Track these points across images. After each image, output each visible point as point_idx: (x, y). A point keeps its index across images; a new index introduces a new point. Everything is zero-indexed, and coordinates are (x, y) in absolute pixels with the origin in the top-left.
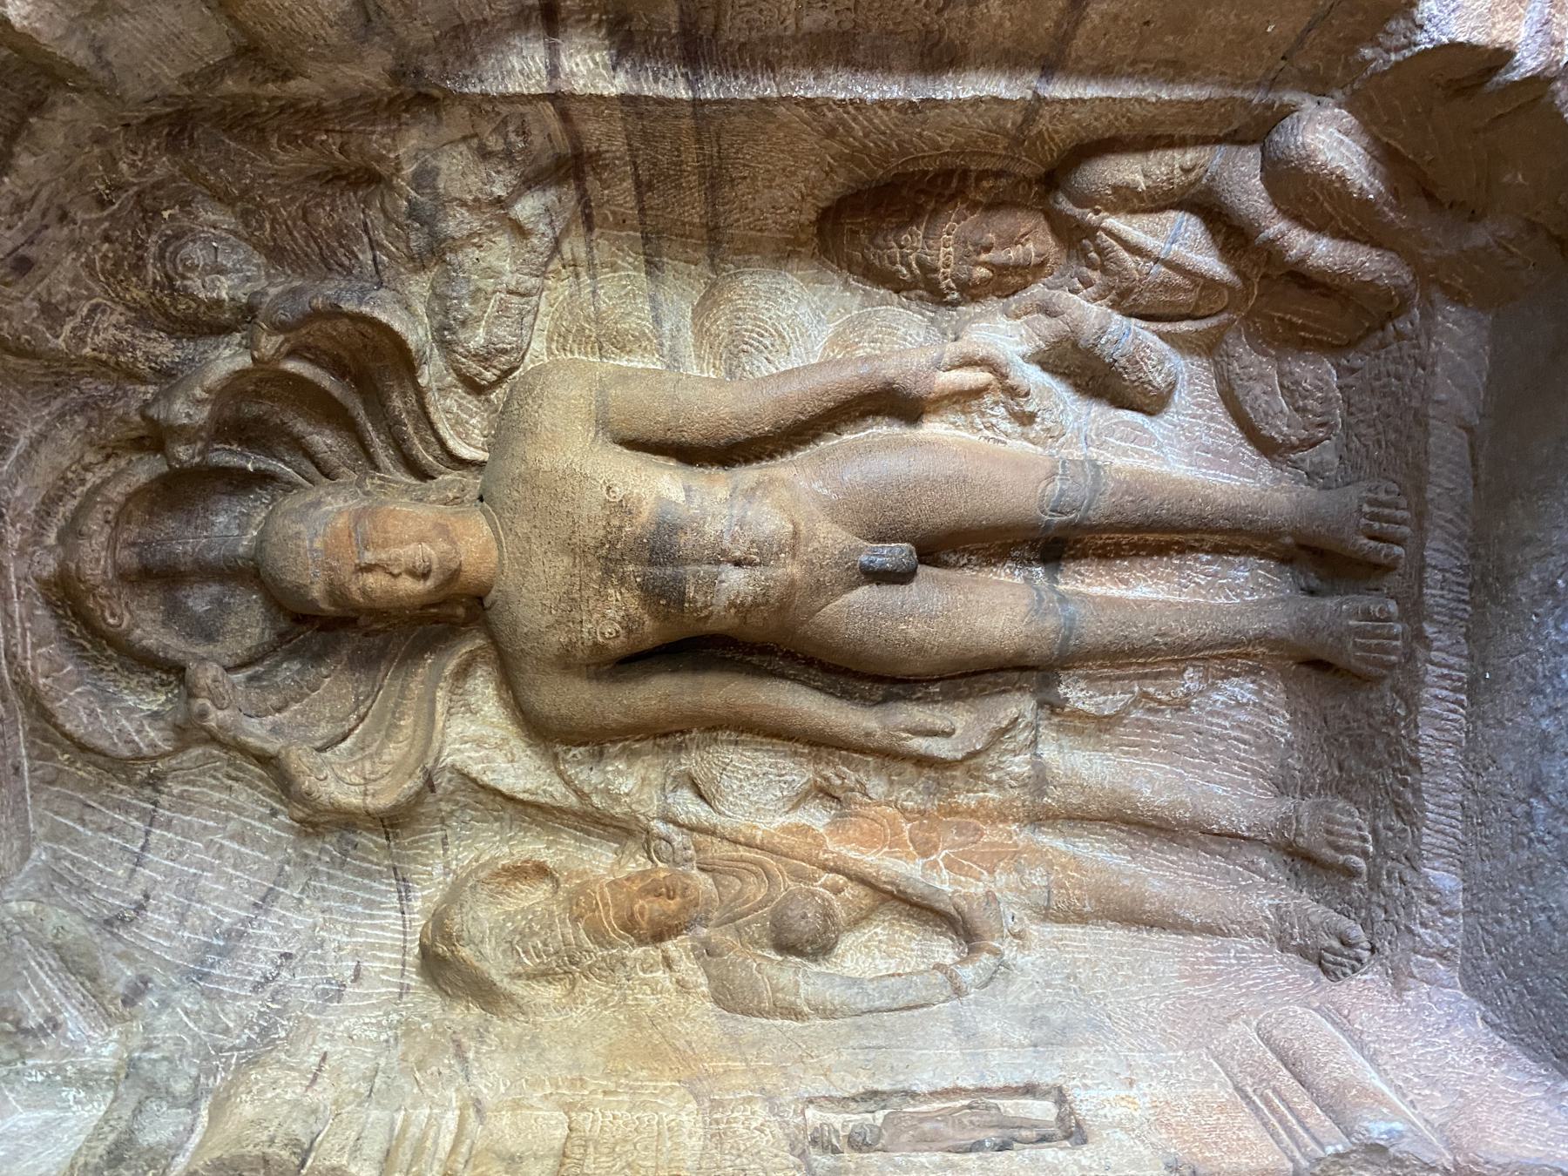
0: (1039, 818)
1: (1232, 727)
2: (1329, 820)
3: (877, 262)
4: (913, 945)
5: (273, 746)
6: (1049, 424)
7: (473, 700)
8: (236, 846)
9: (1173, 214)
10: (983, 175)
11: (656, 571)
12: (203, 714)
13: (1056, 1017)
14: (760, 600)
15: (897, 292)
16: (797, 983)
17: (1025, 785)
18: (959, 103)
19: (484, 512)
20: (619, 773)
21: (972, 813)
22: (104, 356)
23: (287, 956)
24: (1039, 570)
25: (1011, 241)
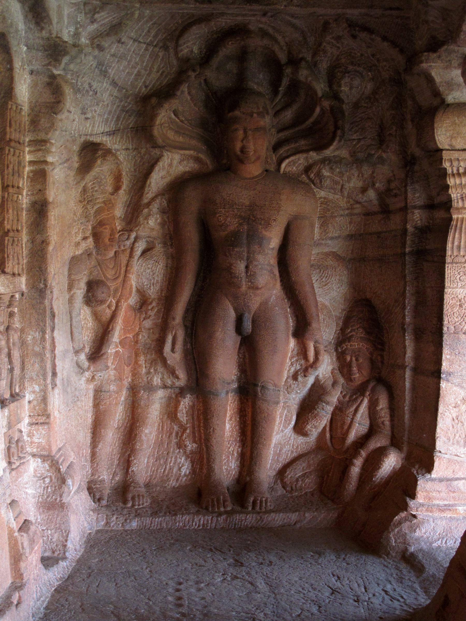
0: (134, 390)
1: (170, 466)
2: (143, 496)
3: (352, 320)
4: (86, 337)
5: (178, 93)
6: (293, 386)
7: (185, 162)
8: (135, 72)
9: (368, 422)
10: (382, 356)
11: (245, 236)
12: (194, 71)
13: (69, 390)
14: (233, 275)
15: (341, 329)
16: (80, 289)
17: (148, 383)
18: (405, 340)
19: (262, 173)
20: (156, 220)
21: (136, 362)
22: (322, 47)
23: (96, 94)
24: (235, 386)
25: (360, 368)
